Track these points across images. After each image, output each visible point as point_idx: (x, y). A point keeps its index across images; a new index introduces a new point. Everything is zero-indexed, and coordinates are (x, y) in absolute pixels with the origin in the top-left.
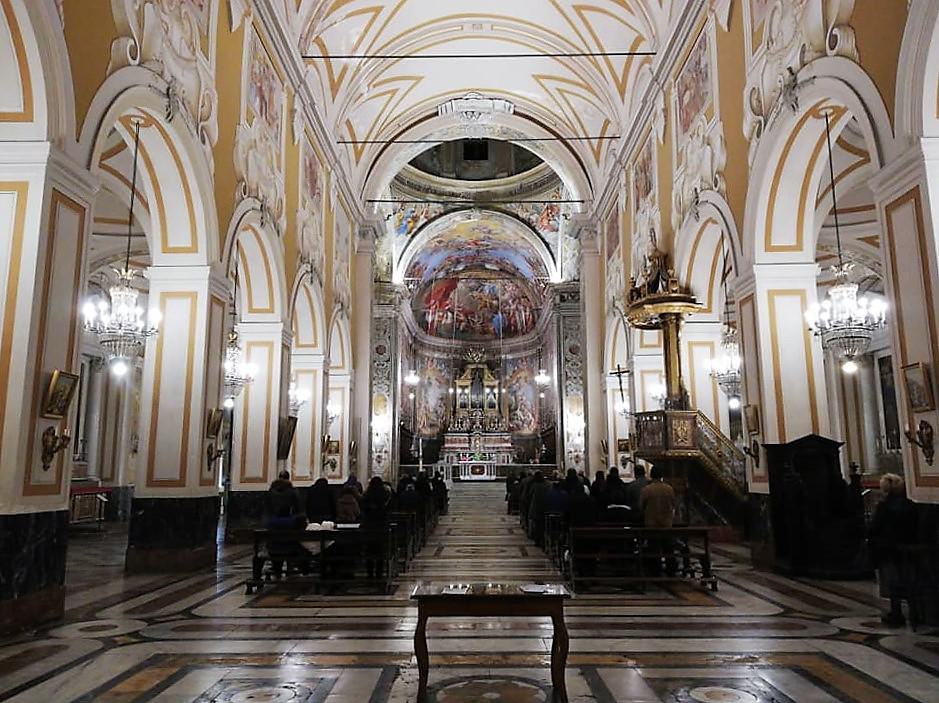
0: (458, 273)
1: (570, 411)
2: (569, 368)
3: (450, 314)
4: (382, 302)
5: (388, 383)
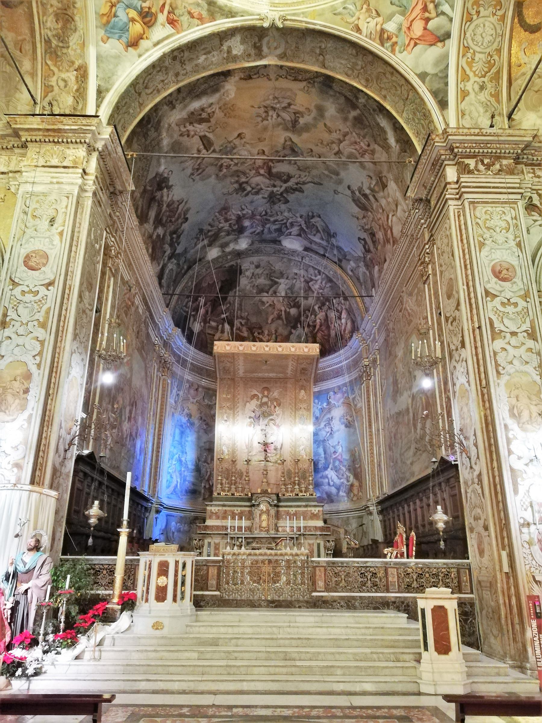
0: (239, 254)
1: (512, 415)
2: (496, 311)
3: (227, 327)
4: (55, 162)
5: (40, 333)
